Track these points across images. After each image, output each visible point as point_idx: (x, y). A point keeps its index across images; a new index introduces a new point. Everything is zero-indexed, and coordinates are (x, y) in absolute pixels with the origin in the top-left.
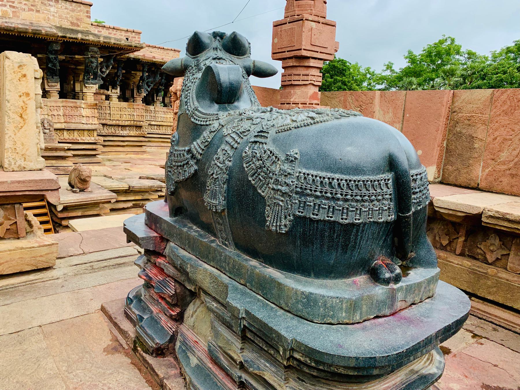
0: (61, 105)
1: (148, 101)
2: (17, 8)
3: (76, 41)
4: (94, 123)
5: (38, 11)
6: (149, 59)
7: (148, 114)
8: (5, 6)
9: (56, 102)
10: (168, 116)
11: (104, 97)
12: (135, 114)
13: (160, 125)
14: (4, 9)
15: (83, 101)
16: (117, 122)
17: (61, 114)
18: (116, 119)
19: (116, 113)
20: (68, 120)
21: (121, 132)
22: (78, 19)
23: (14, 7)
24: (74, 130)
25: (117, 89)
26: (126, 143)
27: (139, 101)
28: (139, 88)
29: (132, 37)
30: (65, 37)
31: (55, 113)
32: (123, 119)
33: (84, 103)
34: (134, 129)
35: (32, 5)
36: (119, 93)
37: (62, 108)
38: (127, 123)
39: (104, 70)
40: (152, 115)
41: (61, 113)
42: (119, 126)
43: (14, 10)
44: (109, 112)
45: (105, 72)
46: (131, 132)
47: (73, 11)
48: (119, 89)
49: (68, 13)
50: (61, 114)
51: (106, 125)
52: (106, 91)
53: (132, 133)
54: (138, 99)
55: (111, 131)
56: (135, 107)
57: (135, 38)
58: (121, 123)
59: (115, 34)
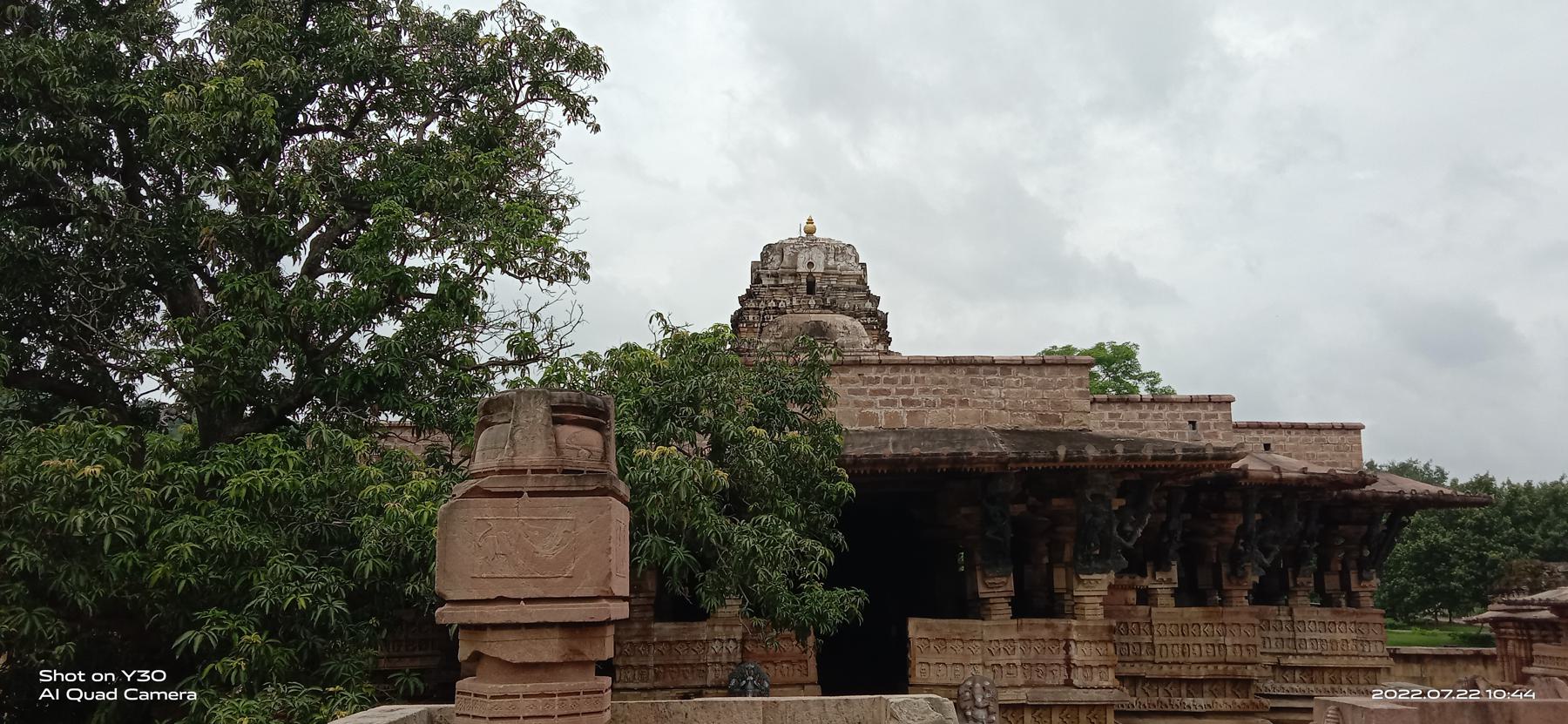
0: (1015, 636)
1: (1268, 593)
2: (919, 403)
3: (1051, 465)
5: (964, 403)
6: (1261, 474)
7: (1272, 634)
8: (894, 403)
9: (1003, 628)
10: (1339, 636)
11: (1132, 596)
12: (1228, 641)
13: (1312, 669)
14: (892, 410)
15: (1074, 623)
16: (1175, 669)
17: (1018, 663)
18: (1170, 659)
19: (1170, 640)
20: (1035, 679)
21: (1189, 701)
22: (1057, 405)
23: (912, 403)
25: (1168, 569)
27: (1241, 599)
28: (1236, 560)
29: (1207, 417)
30: (1026, 460)
31: (1002, 659)
32: (1192, 659)
34: (1228, 691)
35: (950, 392)
36: (1175, 579)
37: (1018, 645)
38: (1203, 672)
39: (1129, 528)
40: (1285, 634)
41: (1016, 659)
42: (1179, 681)
43: (912, 409)
44: (1147, 639)
45: (1133, 533)
46: (1220, 701)
47: (1044, 386)
48: (1174, 568)
49: (1033, 395)
50: (1018, 663)
51: (1145, 680)
52: (1138, 578)
54: (1235, 593)
55: (1158, 698)
56: (1228, 620)
57: (1215, 416)
58: (1184, 673)
59: (1156, 416)
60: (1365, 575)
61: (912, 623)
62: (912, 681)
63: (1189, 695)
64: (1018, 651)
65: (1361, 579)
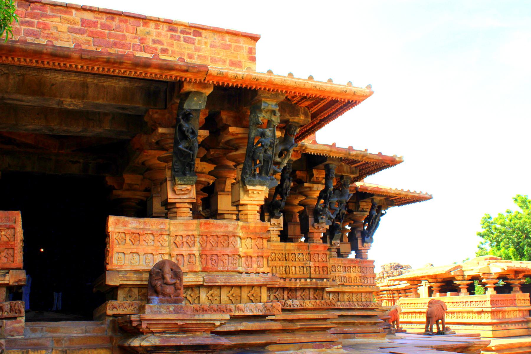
4: (262, 270)
10: (353, 274)
12: (312, 264)
13: (338, 293)
15: (240, 223)
24: (220, 287)
25: (278, 217)
26: (298, 325)
31: (185, 250)
32: (291, 276)
33: (243, 227)
41: (196, 250)
42: (284, 289)
48: (282, 218)
50: (197, 253)
53: (309, 304)
60: (366, 239)
61: (112, 220)
62: (109, 267)
63: (289, 298)
64: (197, 244)
65: (363, 241)
